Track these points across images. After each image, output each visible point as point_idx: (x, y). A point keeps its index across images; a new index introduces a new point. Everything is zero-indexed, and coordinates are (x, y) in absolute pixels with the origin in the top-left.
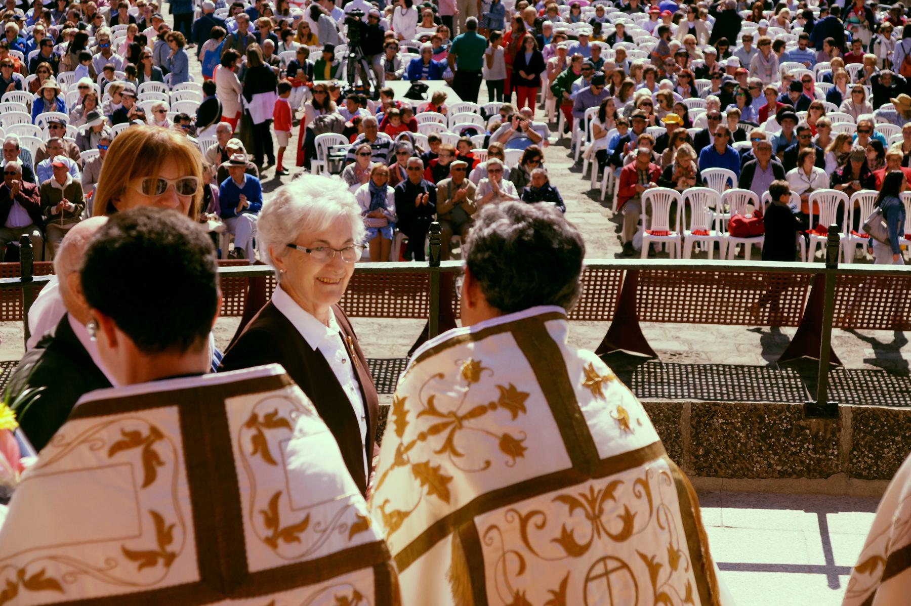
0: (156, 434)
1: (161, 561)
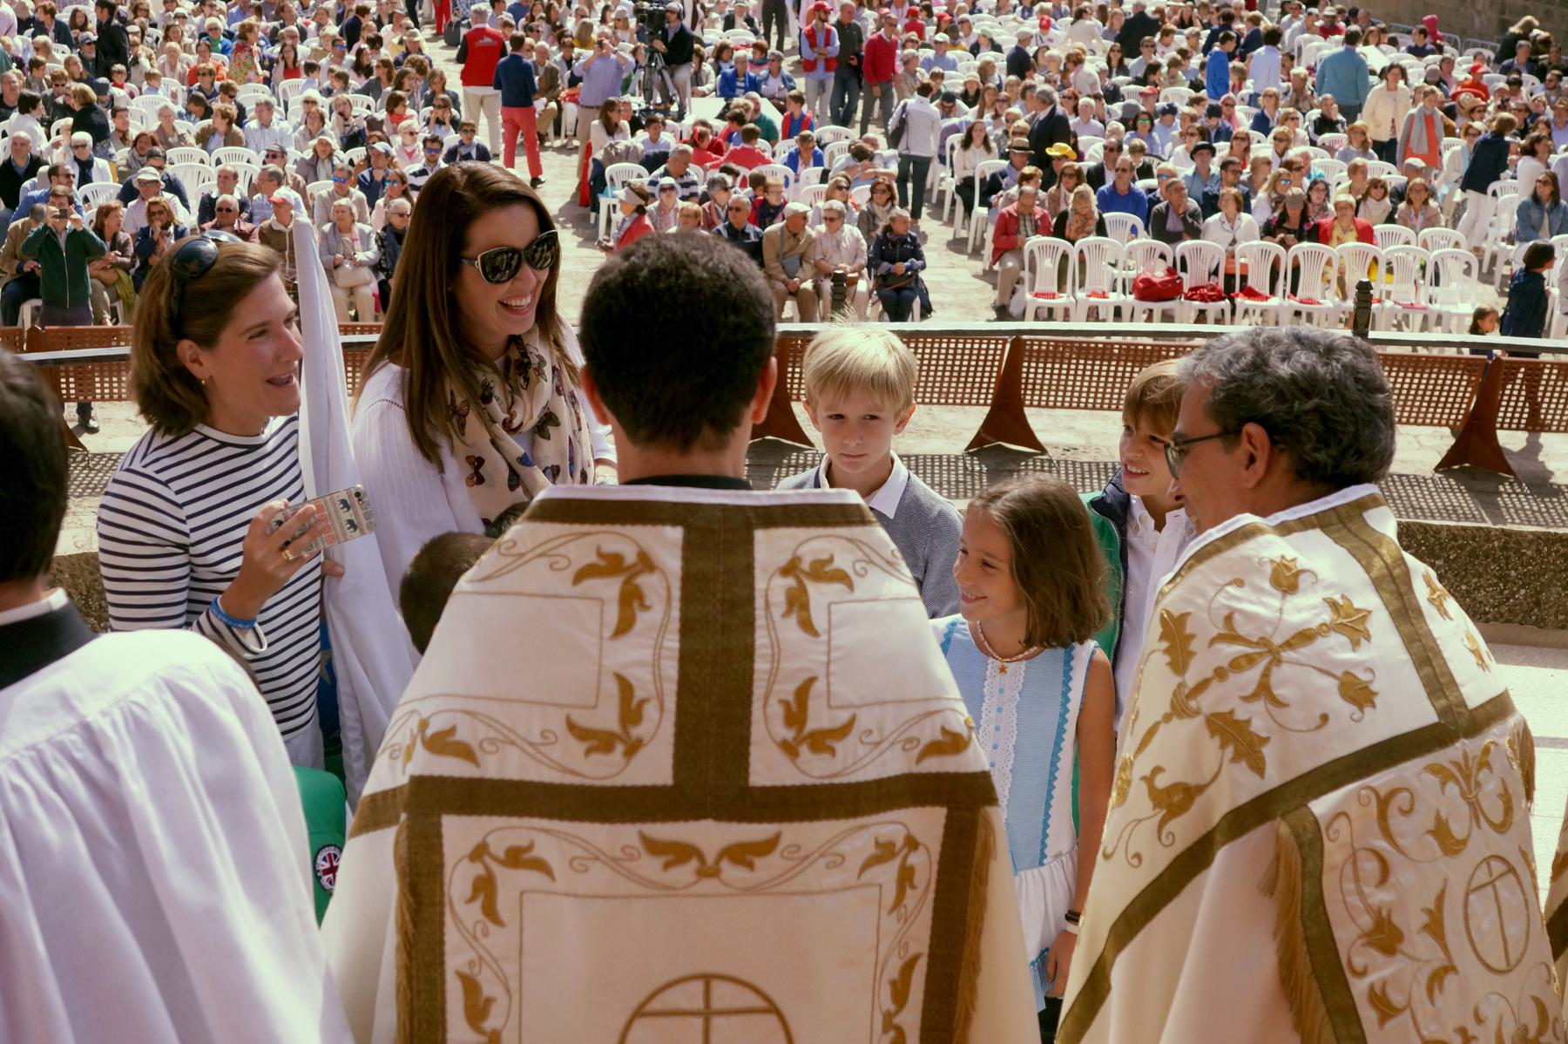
0: (646, 563)
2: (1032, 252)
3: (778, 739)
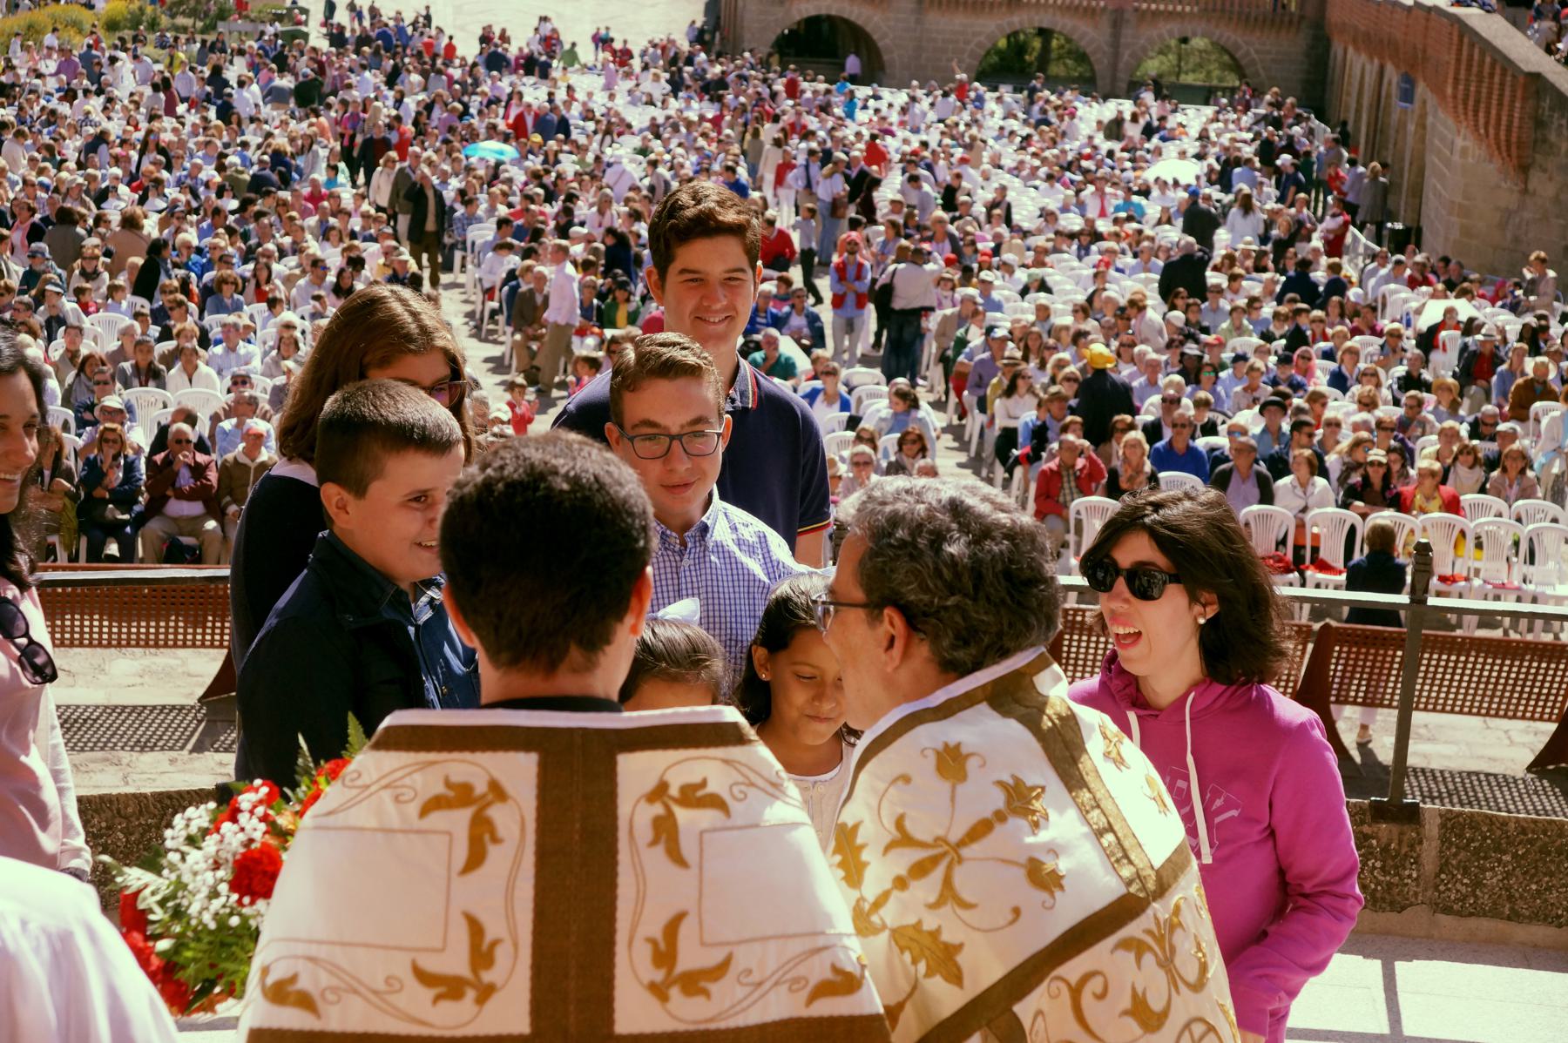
2: (1078, 513)
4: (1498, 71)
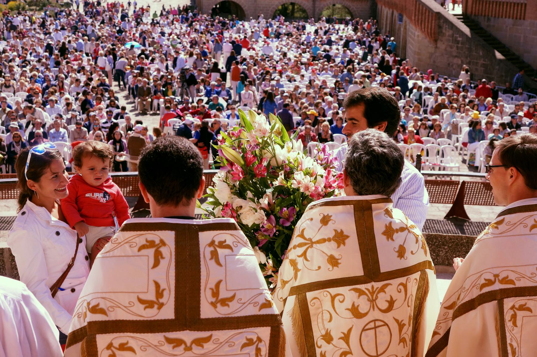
1: (156, 306)
3: (210, 301)
4: (427, 12)
